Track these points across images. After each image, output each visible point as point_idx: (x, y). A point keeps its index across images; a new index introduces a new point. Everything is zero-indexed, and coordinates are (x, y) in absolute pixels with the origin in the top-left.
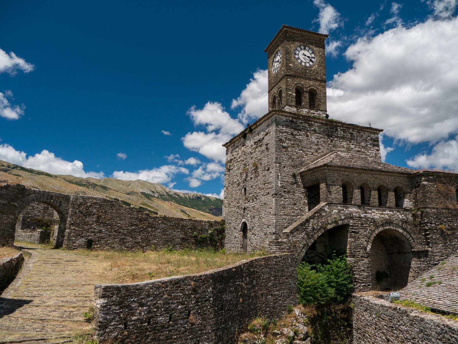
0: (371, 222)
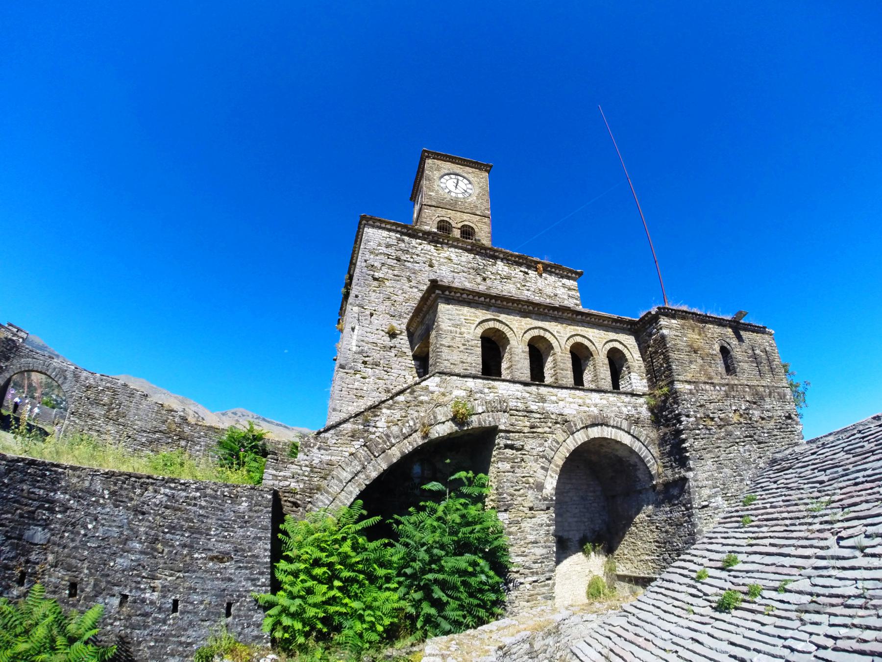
0: (556, 423)
